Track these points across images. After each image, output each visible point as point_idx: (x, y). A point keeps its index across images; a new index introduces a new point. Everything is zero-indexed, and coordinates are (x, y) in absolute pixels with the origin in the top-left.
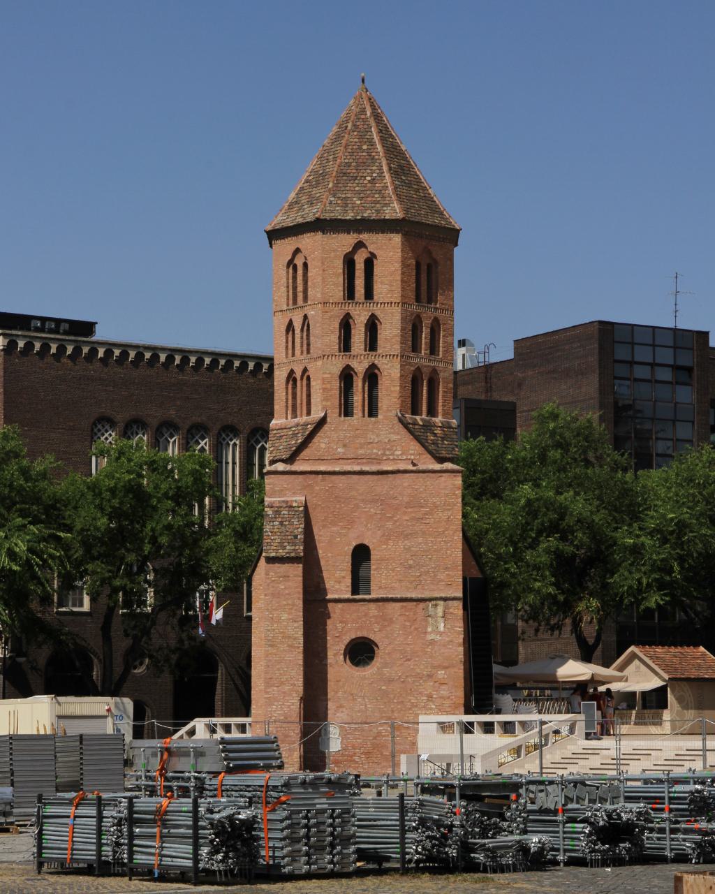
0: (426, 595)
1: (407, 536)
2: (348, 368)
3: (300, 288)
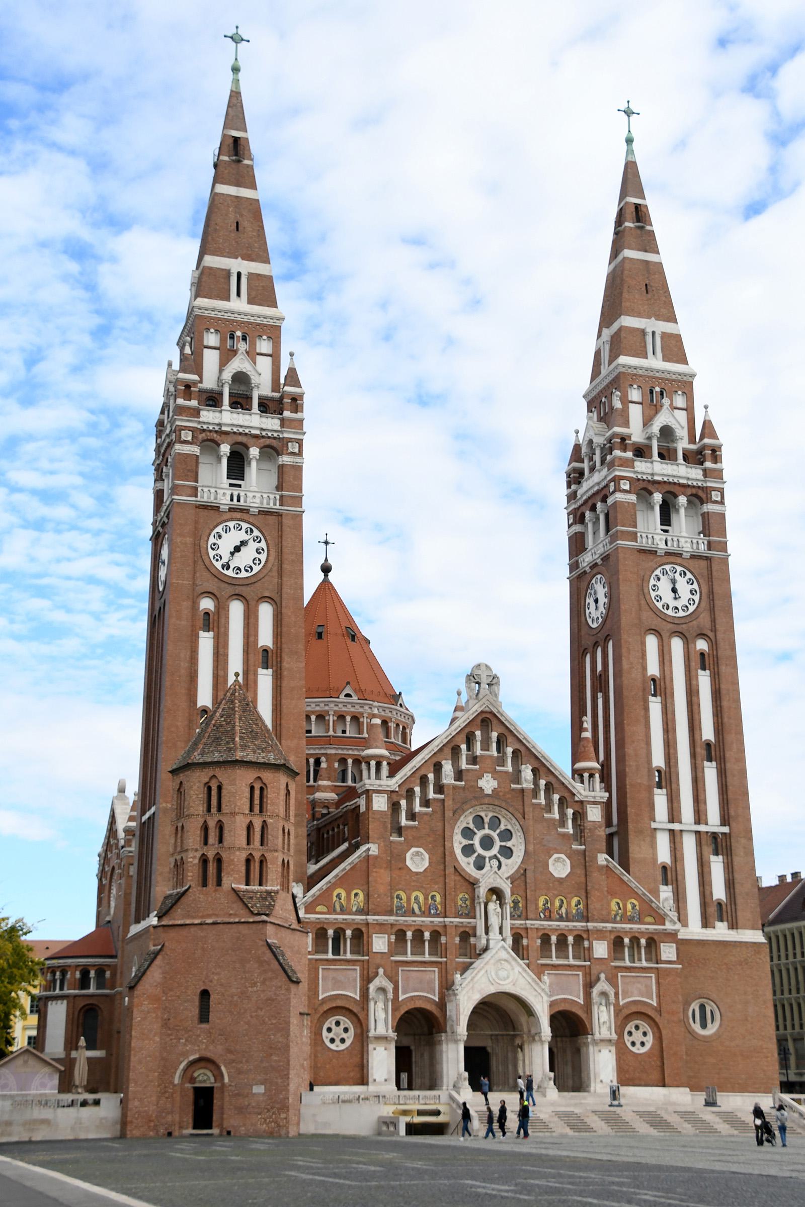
3: (257, 801)
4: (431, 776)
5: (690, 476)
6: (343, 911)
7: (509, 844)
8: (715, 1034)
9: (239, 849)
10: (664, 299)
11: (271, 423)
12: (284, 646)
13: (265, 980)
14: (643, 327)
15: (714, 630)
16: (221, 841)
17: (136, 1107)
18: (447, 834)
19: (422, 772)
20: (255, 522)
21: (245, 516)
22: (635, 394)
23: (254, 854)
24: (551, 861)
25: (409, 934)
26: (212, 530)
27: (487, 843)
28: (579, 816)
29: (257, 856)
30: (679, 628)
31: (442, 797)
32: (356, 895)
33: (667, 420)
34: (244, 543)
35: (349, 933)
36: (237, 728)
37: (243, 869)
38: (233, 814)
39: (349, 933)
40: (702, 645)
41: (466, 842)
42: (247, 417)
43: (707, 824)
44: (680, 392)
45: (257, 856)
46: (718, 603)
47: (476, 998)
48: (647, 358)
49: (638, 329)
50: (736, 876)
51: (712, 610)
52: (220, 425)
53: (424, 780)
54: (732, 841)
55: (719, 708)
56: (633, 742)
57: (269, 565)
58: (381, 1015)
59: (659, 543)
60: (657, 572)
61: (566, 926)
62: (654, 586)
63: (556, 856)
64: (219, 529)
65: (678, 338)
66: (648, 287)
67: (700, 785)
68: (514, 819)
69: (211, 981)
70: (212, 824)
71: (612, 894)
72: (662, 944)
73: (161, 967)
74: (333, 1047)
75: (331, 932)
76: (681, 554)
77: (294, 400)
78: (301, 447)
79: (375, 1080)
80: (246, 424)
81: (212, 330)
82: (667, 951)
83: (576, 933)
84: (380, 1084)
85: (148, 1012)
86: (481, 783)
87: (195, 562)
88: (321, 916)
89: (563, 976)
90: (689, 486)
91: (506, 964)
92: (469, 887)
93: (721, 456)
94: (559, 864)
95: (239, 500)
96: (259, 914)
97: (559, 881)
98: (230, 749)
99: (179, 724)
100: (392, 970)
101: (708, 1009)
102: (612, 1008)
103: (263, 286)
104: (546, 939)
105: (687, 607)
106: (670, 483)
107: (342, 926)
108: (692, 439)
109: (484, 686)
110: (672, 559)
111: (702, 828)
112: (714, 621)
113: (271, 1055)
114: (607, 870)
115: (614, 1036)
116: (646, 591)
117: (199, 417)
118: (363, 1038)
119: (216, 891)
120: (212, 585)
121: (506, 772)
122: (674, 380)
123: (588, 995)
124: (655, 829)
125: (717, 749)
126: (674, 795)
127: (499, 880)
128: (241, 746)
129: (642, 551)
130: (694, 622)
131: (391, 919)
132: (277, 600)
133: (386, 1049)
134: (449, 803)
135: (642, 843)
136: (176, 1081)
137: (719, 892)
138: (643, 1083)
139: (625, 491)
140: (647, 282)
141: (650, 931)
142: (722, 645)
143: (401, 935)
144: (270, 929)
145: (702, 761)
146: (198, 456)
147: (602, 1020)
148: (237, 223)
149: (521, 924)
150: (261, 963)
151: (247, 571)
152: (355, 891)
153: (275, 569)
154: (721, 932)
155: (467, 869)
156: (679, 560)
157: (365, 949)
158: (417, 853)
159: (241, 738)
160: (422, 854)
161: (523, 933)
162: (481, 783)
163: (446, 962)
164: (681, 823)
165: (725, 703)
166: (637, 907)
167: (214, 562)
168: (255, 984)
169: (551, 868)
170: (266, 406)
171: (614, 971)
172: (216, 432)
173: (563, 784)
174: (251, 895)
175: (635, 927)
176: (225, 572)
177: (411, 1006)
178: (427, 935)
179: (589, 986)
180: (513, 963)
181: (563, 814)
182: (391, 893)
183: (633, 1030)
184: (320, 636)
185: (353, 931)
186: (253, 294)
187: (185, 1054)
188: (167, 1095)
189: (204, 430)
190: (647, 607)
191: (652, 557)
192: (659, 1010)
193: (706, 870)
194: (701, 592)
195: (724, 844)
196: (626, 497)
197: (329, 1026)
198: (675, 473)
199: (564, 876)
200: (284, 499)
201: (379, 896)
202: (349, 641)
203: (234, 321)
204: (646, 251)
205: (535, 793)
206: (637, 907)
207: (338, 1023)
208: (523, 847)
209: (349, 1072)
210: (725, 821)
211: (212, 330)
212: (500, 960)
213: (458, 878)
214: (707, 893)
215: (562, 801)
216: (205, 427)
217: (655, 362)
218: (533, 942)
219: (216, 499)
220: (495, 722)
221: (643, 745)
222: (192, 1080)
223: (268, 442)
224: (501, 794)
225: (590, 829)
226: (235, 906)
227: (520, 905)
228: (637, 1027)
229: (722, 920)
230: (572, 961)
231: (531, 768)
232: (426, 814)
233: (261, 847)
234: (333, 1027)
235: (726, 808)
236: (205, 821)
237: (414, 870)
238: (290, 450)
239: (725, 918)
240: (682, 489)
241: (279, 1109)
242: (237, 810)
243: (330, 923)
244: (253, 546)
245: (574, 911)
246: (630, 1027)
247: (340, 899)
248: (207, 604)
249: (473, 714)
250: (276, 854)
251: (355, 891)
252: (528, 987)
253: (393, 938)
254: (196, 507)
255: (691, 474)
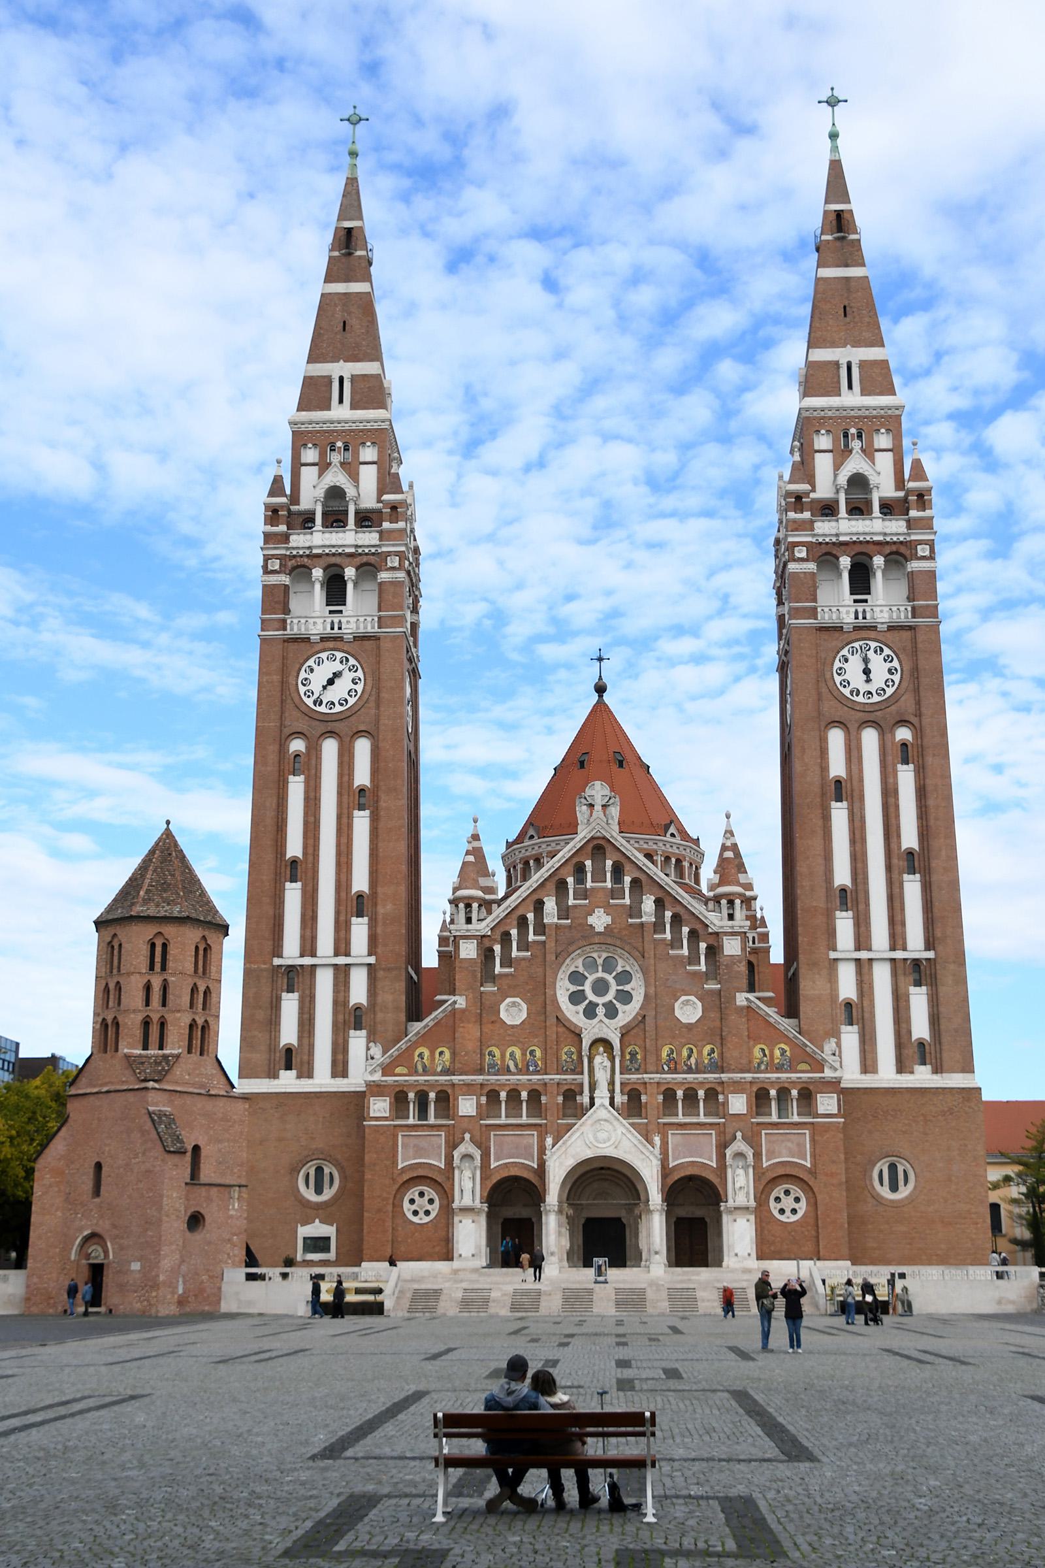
0: (227, 1182)
1: (220, 1141)
2: (194, 1020)
3: (158, 959)
4: (530, 916)
5: (888, 531)
6: (425, 1072)
7: (627, 988)
8: (907, 1198)
9: (134, 1011)
10: (867, 319)
11: (369, 538)
12: (381, 783)
13: (145, 1150)
14: (835, 359)
15: (919, 714)
16: (119, 1004)
17: (35, 1284)
18: (549, 980)
19: (520, 912)
20: (350, 650)
21: (339, 644)
22: (823, 441)
23: (151, 1015)
24: (677, 1005)
25: (503, 1095)
26: (302, 665)
27: (601, 987)
28: (713, 951)
29: (155, 1017)
30: (872, 717)
31: (543, 938)
32: (441, 1053)
33: (858, 467)
34: (337, 675)
35: (432, 1095)
36: (147, 881)
37: (138, 1033)
38: (129, 974)
39: (432, 1095)
40: (903, 734)
41: (573, 988)
42: (341, 535)
43: (905, 949)
44: (883, 430)
45: (155, 1017)
46: (924, 681)
47: (571, 1162)
48: (840, 395)
49: (830, 362)
50: (942, 1009)
51: (917, 691)
52: (310, 548)
53: (522, 922)
54: (938, 967)
55: (923, 809)
56: (808, 858)
57: (366, 696)
58: (468, 1185)
59: (845, 616)
60: (845, 652)
61: (694, 1079)
62: (840, 669)
63: (684, 998)
64: (311, 662)
65: (884, 364)
66: (848, 309)
67: (897, 904)
68: (632, 959)
69: (103, 1153)
70: (112, 986)
71: (754, 1038)
72: (818, 1095)
73: (65, 1139)
74: (415, 1219)
75: (411, 1095)
76: (876, 627)
77: (394, 508)
78: (265, 567)
79: (460, 1256)
80: (340, 543)
81: (310, 445)
82: (825, 1103)
83: (707, 1086)
84: (466, 1259)
85: (50, 1186)
86: (591, 920)
87: (282, 701)
88: (401, 1077)
89: (692, 1137)
90: (887, 543)
91: (607, 1124)
92: (576, 1039)
93: (930, 500)
94: (688, 1007)
95: (340, 628)
96: (146, 1080)
97: (687, 1027)
98: (133, 904)
99: (264, 878)
100: (481, 1136)
101: (900, 1169)
102: (751, 1170)
103: (369, 387)
104: (669, 1095)
105: (884, 690)
106: (861, 542)
107: (425, 1088)
108: (900, 483)
109: (598, 808)
110: (864, 634)
111: (899, 955)
112: (918, 703)
113: (147, 1230)
114: (748, 1012)
115: (752, 1203)
116: (828, 676)
117: (288, 543)
118: (448, 1211)
119: (112, 1057)
120: (302, 725)
121: (623, 906)
122: (875, 417)
123: (721, 1157)
124: (836, 960)
125: (922, 859)
126: (862, 917)
127: (605, 1030)
128: (144, 900)
129: (823, 629)
130: (893, 707)
131: (480, 1078)
132: (375, 734)
133: (473, 1222)
134: (551, 945)
135: (817, 976)
136: (73, 1257)
137: (920, 1029)
138: (793, 1257)
139: (802, 560)
140: (846, 304)
141: (803, 1080)
142: (928, 731)
143: (493, 1096)
144: (151, 1096)
145: (901, 874)
146: (286, 586)
147: (738, 1185)
148: (344, 323)
149: (638, 1079)
150: (143, 1133)
151: (341, 705)
152: (440, 1050)
153: (373, 698)
154: (922, 1076)
155: (574, 1020)
156: (872, 634)
157: (451, 1112)
158: (514, 1004)
159: (148, 891)
160: (519, 1004)
161: (641, 1089)
162: (591, 920)
163: (546, 1124)
164: (870, 950)
165: (931, 802)
166: (788, 1053)
167: (305, 699)
168: (136, 1156)
169: (678, 1013)
170: (366, 519)
171: (755, 1129)
172: (308, 556)
173: (694, 914)
174: (144, 1060)
175: (784, 1076)
176: (318, 709)
177: (505, 1174)
178: (524, 1095)
179: (722, 1146)
180: (615, 1123)
181: (694, 948)
182: (481, 1050)
183: (782, 1196)
184: (582, 764)
185: (508, 1093)
186: (357, 397)
187: (81, 1230)
188: (65, 1272)
189: (294, 556)
190: (830, 696)
191: (837, 634)
192: (812, 1172)
193: (902, 1004)
194: (902, 670)
195: (928, 972)
196: (801, 566)
197: (412, 1197)
198: (867, 530)
199: (693, 1021)
200: (382, 619)
201: (465, 1055)
202: (615, 767)
203: (333, 431)
204: (847, 266)
205: (659, 926)
206: (788, 1053)
207: (422, 1194)
208: (642, 991)
209: (434, 1247)
210: (928, 947)
211: (310, 445)
212: (599, 1120)
213: (561, 1029)
214: (903, 1032)
215: (693, 934)
216: (295, 552)
217: (851, 399)
218: (652, 1099)
219: (307, 629)
220: (609, 849)
221: (820, 861)
222: (88, 1256)
223: (365, 559)
224: (616, 931)
225: (727, 966)
226: (127, 1072)
227: (639, 1057)
228: (787, 1193)
229: (924, 1063)
230: (702, 1119)
231: (653, 898)
232: (524, 959)
233: (161, 1008)
234: (416, 1197)
235: (930, 928)
236: (107, 984)
237: (509, 1023)
238: (389, 565)
239: (928, 1061)
240: (877, 548)
241: (151, 1287)
242: (132, 970)
243: (411, 1085)
244: (348, 676)
245: (706, 1061)
246: (778, 1191)
247: (423, 1058)
248: (297, 745)
249: (580, 841)
250: (178, 1015)
251: (440, 1050)
252: (633, 1149)
253: (484, 1100)
254: (284, 641)
255: (895, 527)
